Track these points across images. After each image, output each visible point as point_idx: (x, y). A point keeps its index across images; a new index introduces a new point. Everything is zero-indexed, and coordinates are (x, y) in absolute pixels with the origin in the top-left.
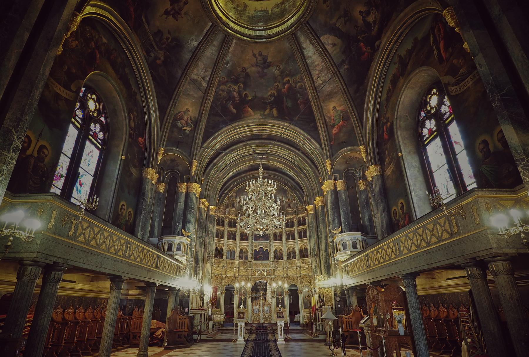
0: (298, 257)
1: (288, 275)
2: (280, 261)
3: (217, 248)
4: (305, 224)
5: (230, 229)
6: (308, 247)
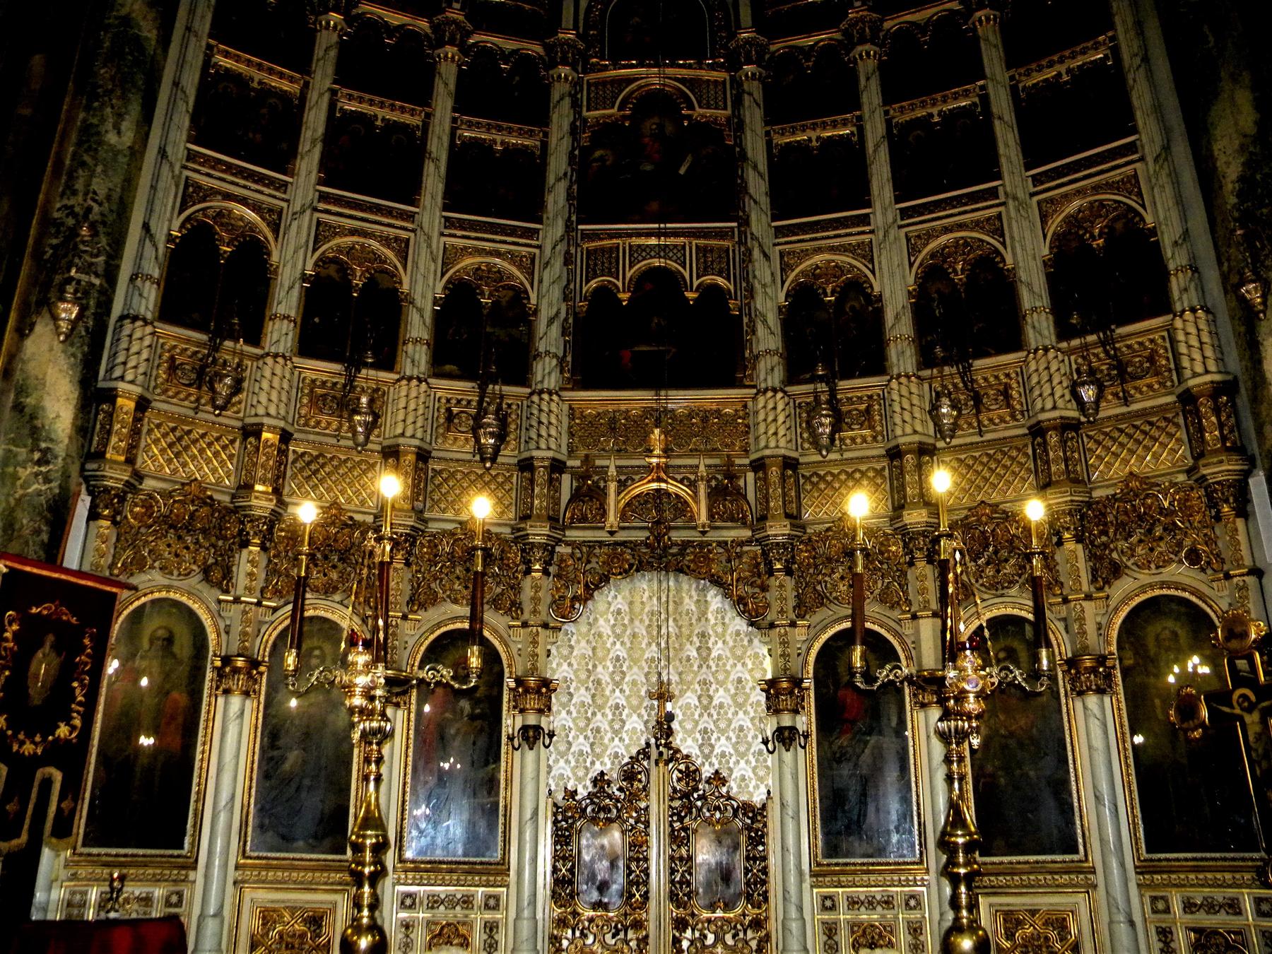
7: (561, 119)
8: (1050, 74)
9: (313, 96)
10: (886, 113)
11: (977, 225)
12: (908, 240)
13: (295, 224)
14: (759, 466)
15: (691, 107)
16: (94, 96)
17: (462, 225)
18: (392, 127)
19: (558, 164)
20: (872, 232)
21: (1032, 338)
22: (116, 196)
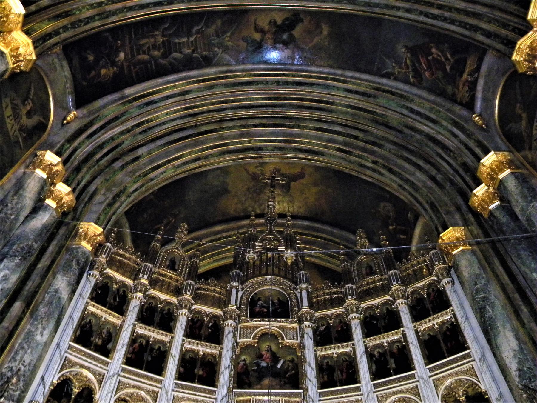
5: (142, 330)
7: (228, 341)
8: (430, 325)
9: (126, 326)
10: (364, 342)
11: (407, 391)
12: (378, 398)
13: (109, 381)
15: (283, 339)
16: (35, 319)
17: (182, 387)
18: (157, 341)
19: (226, 362)
20: (362, 395)
22: (33, 364)
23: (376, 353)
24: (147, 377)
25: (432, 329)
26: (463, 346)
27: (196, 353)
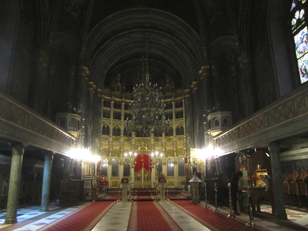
0: (174, 134)
1: (165, 149)
2: (160, 138)
3: (104, 127)
4: (181, 106)
6: (184, 126)
8: (178, 110)
14: (151, 145)
21: (174, 135)
23: (166, 114)
24: (118, 121)
25: (178, 111)
26: (182, 117)
27: (127, 113)
